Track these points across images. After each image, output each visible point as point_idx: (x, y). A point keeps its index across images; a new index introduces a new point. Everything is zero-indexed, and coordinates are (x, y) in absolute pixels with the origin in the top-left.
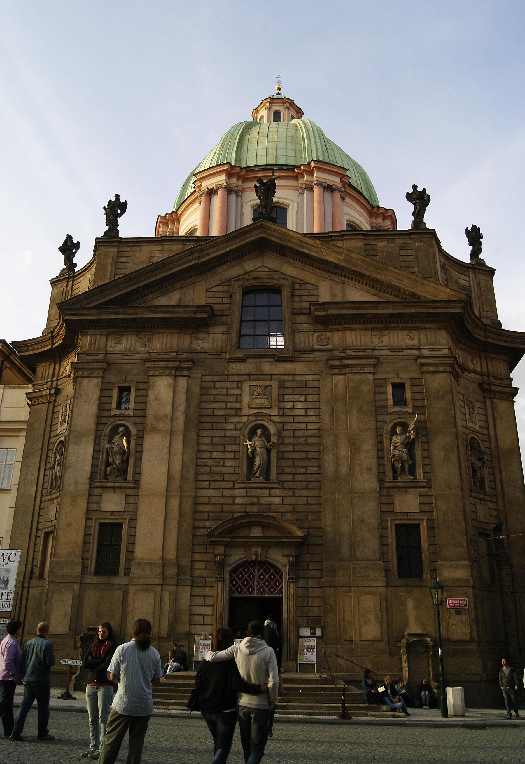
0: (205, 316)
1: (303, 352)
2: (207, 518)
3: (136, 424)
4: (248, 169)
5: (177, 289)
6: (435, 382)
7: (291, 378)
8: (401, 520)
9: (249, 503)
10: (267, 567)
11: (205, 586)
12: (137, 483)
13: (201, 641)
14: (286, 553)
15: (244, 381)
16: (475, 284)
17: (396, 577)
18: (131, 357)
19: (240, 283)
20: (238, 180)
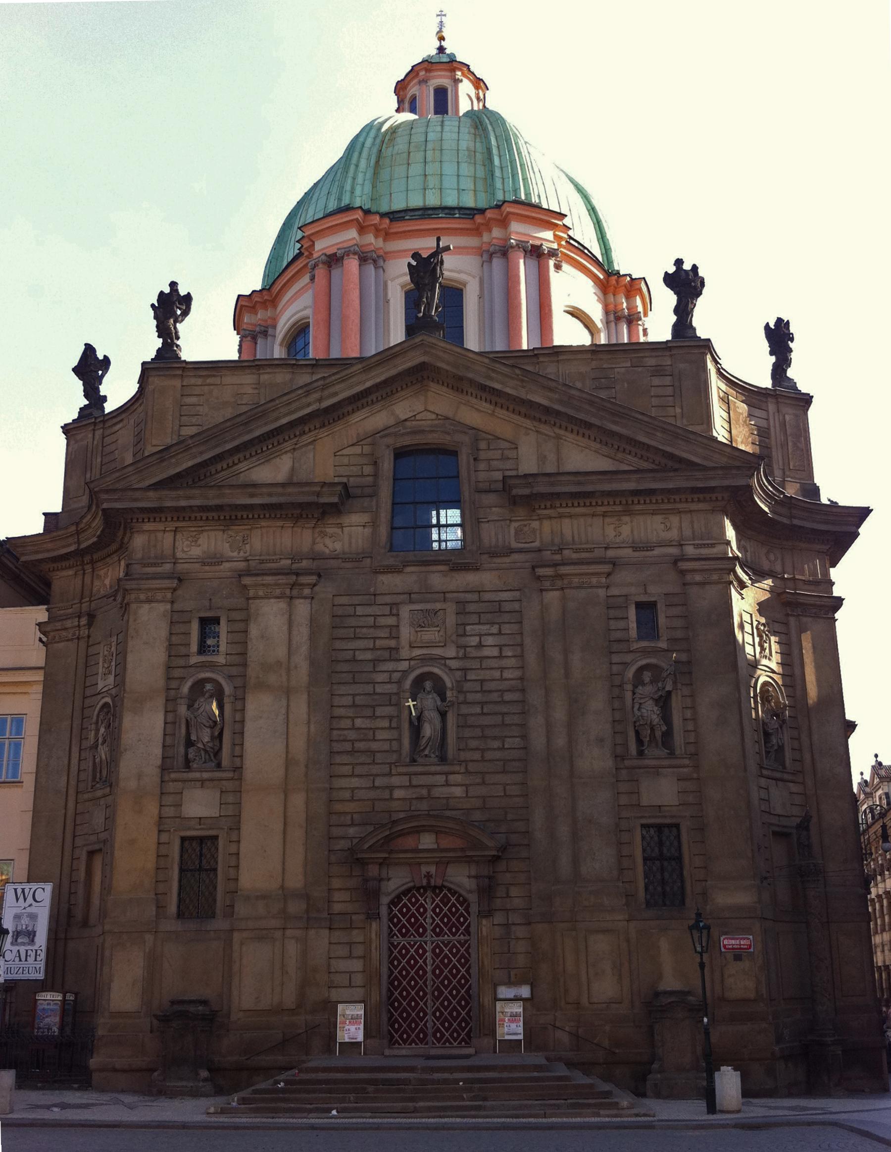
0: (335, 500)
1: (494, 554)
2: (350, 823)
3: (230, 677)
4: (394, 216)
5: (286, 452)
7: (475, 597)
8: (650, 817)
10: (445, 895)
11: (351, 928)
12: (238, 769)
13: (348, 1012)
14: (473, 873)
16: (777, 425)
17: (644, 906)
18: (217, 568)
19: (390, 440)
20: (376, 237)
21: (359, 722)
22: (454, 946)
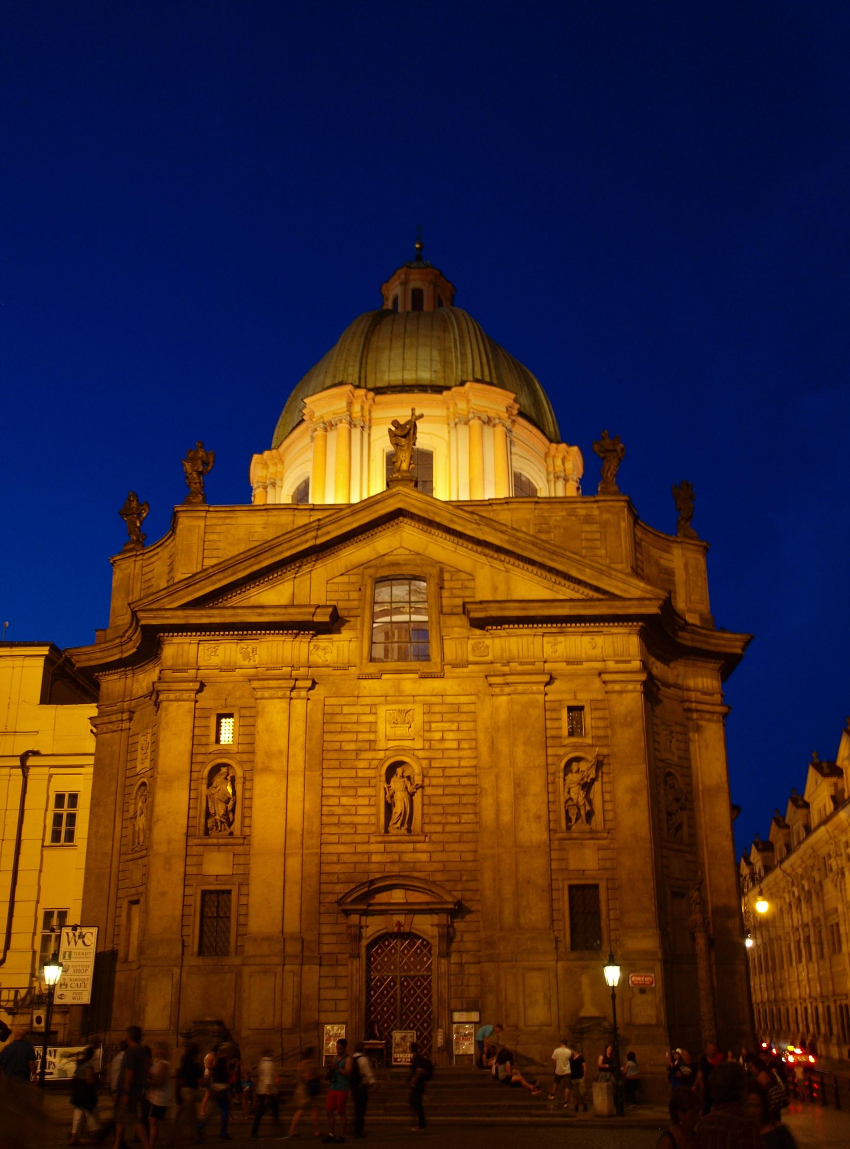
3: (241, 763)
6: (622, 704)
9: (388, 860)
14: (436, 922)
17: (569, 950)
19: (371, 571)
22: (419, 980)
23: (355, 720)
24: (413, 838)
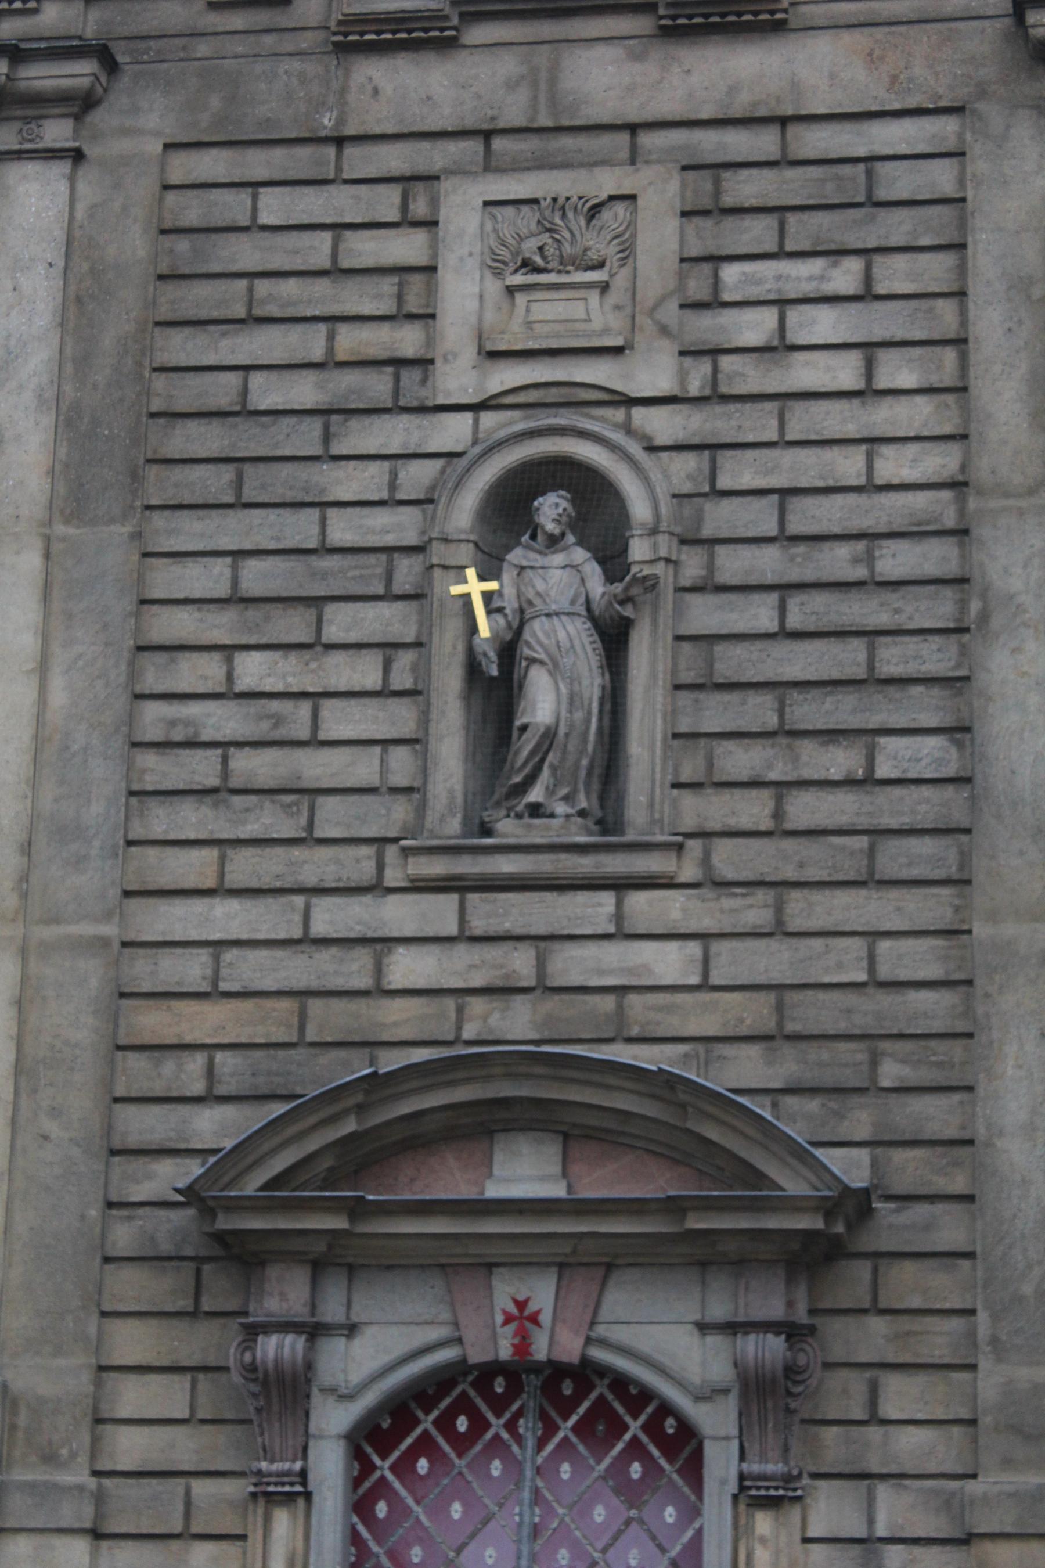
9: (477, 980)
14: (719, 1310)
15: (450, 172)
21: (254, 670)
23: (321, 260)
24: (616, 864)
